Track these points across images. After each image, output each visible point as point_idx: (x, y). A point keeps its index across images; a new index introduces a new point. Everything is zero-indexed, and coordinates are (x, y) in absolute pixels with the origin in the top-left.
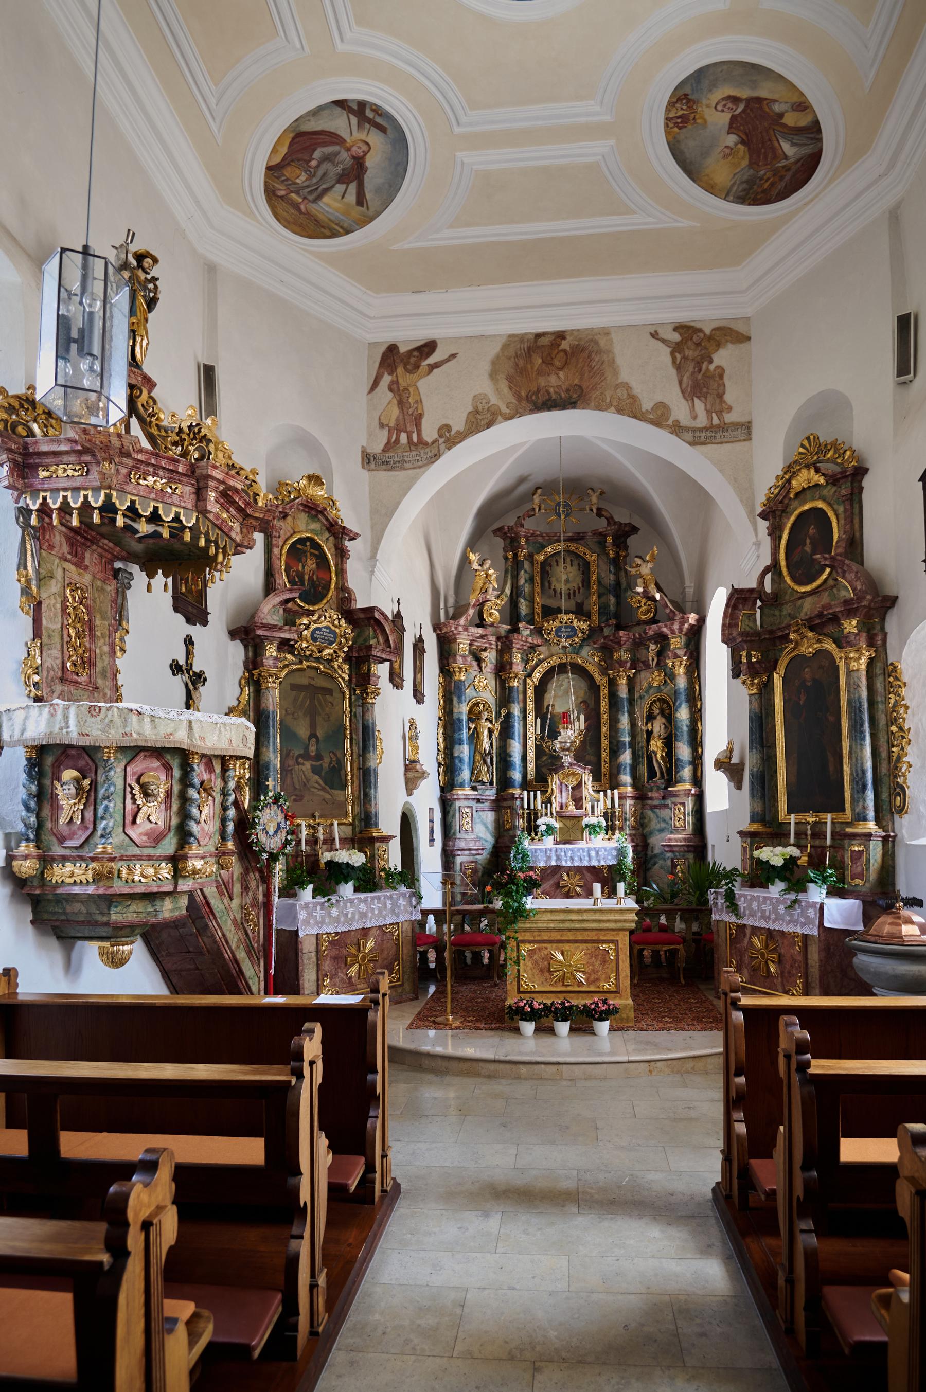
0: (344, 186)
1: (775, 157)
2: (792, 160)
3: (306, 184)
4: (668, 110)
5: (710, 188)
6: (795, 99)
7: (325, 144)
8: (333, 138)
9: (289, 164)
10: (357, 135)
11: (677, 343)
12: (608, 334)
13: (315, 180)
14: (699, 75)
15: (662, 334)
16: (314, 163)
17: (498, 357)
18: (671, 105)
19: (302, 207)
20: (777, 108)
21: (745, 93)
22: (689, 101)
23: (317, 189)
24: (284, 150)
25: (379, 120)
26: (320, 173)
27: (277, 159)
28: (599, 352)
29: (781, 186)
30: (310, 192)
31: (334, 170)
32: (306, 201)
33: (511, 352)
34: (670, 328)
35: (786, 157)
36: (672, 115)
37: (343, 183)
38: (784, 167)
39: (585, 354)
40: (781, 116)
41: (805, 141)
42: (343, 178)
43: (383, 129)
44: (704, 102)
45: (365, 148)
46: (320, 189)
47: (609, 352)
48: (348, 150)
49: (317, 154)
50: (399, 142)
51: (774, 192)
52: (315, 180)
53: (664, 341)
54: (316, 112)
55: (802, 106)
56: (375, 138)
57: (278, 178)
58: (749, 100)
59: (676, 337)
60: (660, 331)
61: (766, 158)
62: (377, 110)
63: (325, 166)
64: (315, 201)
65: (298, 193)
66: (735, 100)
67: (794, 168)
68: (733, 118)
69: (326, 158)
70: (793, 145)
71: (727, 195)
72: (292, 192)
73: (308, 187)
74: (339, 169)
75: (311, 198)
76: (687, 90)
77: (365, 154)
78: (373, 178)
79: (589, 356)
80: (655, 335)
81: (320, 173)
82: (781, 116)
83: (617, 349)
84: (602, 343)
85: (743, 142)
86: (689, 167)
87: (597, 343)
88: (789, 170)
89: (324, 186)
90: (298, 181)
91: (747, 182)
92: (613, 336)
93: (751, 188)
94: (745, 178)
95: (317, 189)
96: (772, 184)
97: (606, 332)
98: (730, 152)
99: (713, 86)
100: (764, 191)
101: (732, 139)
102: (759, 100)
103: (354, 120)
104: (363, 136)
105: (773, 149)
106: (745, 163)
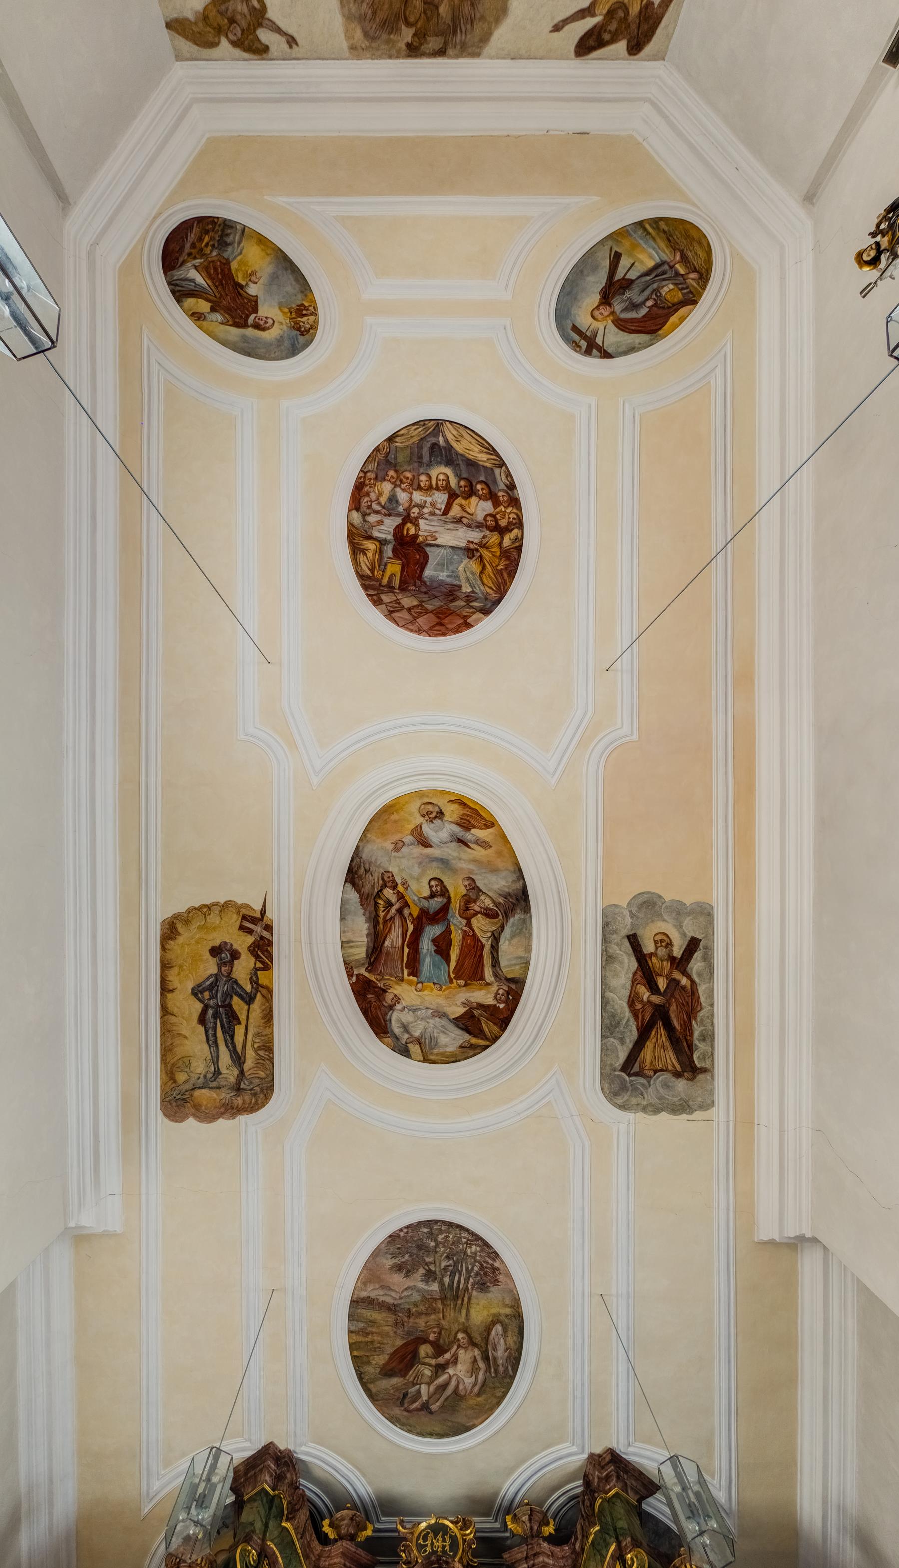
0: (627, 277)
1: (207, 269)
2: (189, 264)
3: (664, 283)
4: (316, 322)
5: (262, 240)
6: (204, 323)
7: (632, 320)
8: (622, 325)
9: (674, 305)
10: (600, 326)
11: (260, 25)
12: (352, 48)
13: (655, 286)
14: (294, 350)
15: (282, 40)
16: (650, 303)
17: (498, 21)
18: (314, 327)
19: (678, 258)
20: (217, 317)
21: (250, 332)
22: (299, 329)
23: (656, 276)
24: (673, 319)
25: (576, 337)
26: (647, 293)
27: (682, 311)
28: (361, 19)
29: (192, 237)
30: (664, 273)
31: (633, 294)
32: (672, 264)
33: (479, 28)
34: (274, 51)
35: (196, 268)
36: (312, 318)
37: (628, 280)
38: (195, 258)
39: (381, 16)
40: (213, 309)
41: (183, 283)
42: (627, 284)
43: (575, 329)
44: (285, 328)
45: (596, 313)
46: (653, 275)
47: (348, 18)
48: (613, 313)
49: (643, 311)
50: (563, 315)
51: (196, 230)
52: (655, 286)
53: (278, 30)
54: (632, 350)
55: (197, 317)
56: (584, 320)
57: (691, 292)
58: (245, 325)
59: (264, 36)
60: (285, 46)
61: (215, 269)
62: (576, 346)
63: (641, 299)
64: (663, 263)
65: (677, 274)
66: (257, 326)
67: (184, 256)
68: (256, 310)
69: (635, 306)
70: (193, 281)
71: (243, 231)
72: (682, 275)
73: (664, 280)
74: (628, 294)
75: (666, 267)
76: (301, 339)
77: (598, 308)
78: (597, 281)
79: (374, 13)
80: (292, 41)
81: (647, 293)
82: (213, 309)
83: (337, 22)
84: (358, 34)
85: (241, 287)
86: (285, 264)
87: (366, 34)
88: (190, 254)
89: (648, 278)
90: (671, 286)
91: (227, 245)
92: (345, 45)
93: (221, 237)
94: (230, 249)
95: (656, 276)
96: (201, 239)
97: (355, 51)
98: (251, 276)
99: (280, 340)
100: (207, 232)
101: (252, 290)
102: (237, 325)
103: (599, 340)
104: (595, 324)
105: (210, 276)
106: (234, 265)
